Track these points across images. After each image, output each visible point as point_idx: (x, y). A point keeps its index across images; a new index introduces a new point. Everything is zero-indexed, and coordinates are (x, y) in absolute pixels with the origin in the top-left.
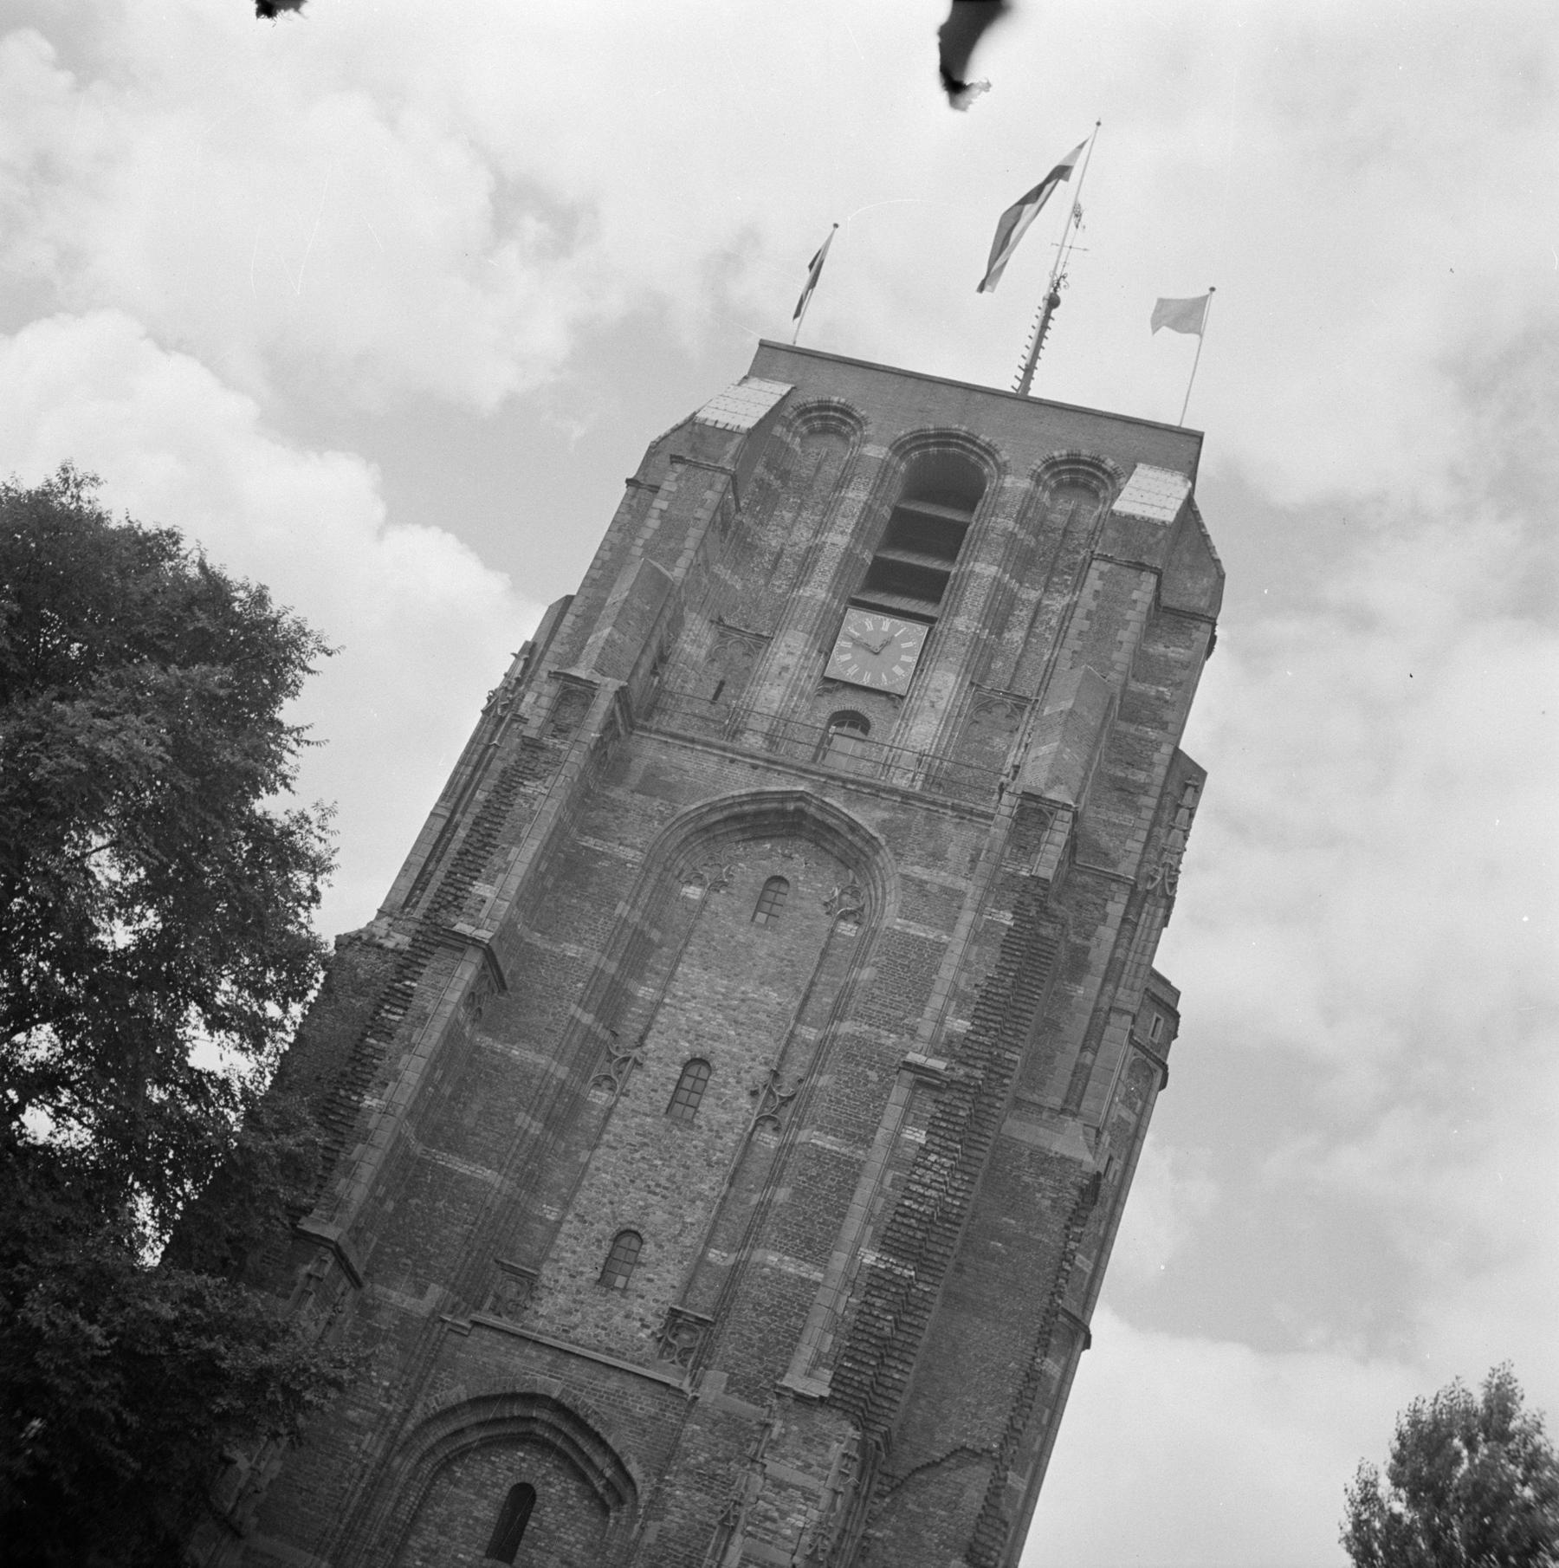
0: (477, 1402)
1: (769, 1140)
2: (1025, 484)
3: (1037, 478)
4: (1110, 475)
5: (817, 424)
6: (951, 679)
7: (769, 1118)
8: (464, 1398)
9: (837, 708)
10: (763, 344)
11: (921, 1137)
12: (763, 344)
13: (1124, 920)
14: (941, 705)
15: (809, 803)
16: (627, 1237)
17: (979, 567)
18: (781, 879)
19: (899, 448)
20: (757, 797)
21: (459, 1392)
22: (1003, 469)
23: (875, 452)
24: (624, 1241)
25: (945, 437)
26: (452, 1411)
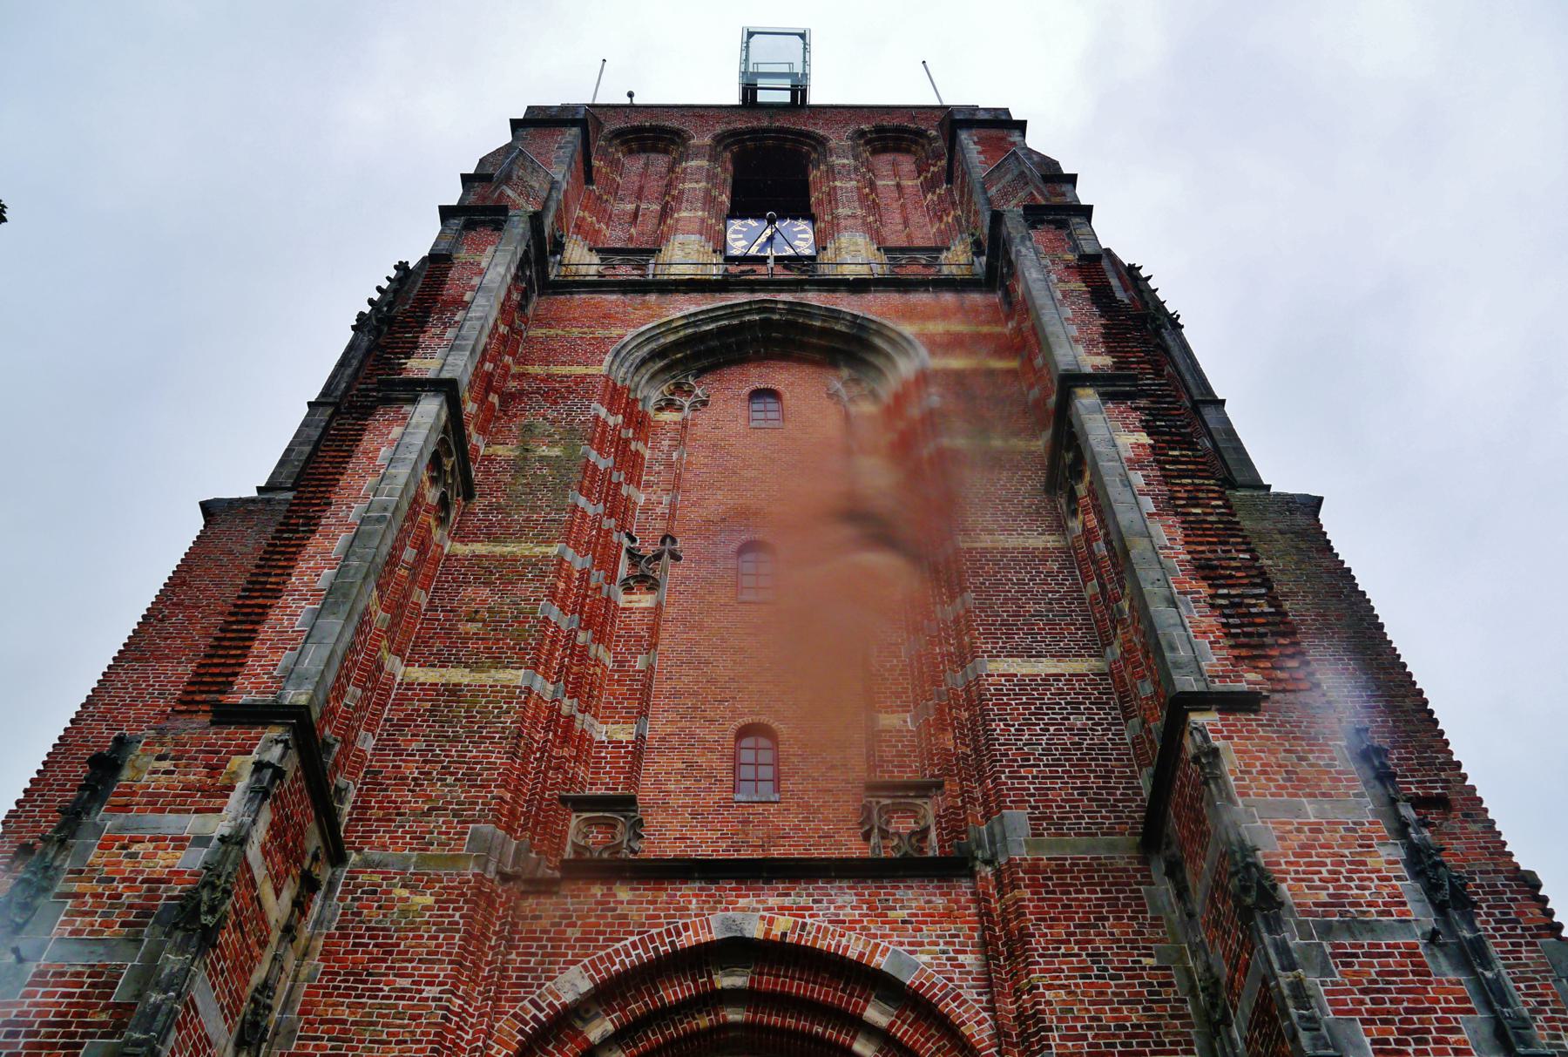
8: (585, 986)
15: (773, 311)
21: (573, 984)
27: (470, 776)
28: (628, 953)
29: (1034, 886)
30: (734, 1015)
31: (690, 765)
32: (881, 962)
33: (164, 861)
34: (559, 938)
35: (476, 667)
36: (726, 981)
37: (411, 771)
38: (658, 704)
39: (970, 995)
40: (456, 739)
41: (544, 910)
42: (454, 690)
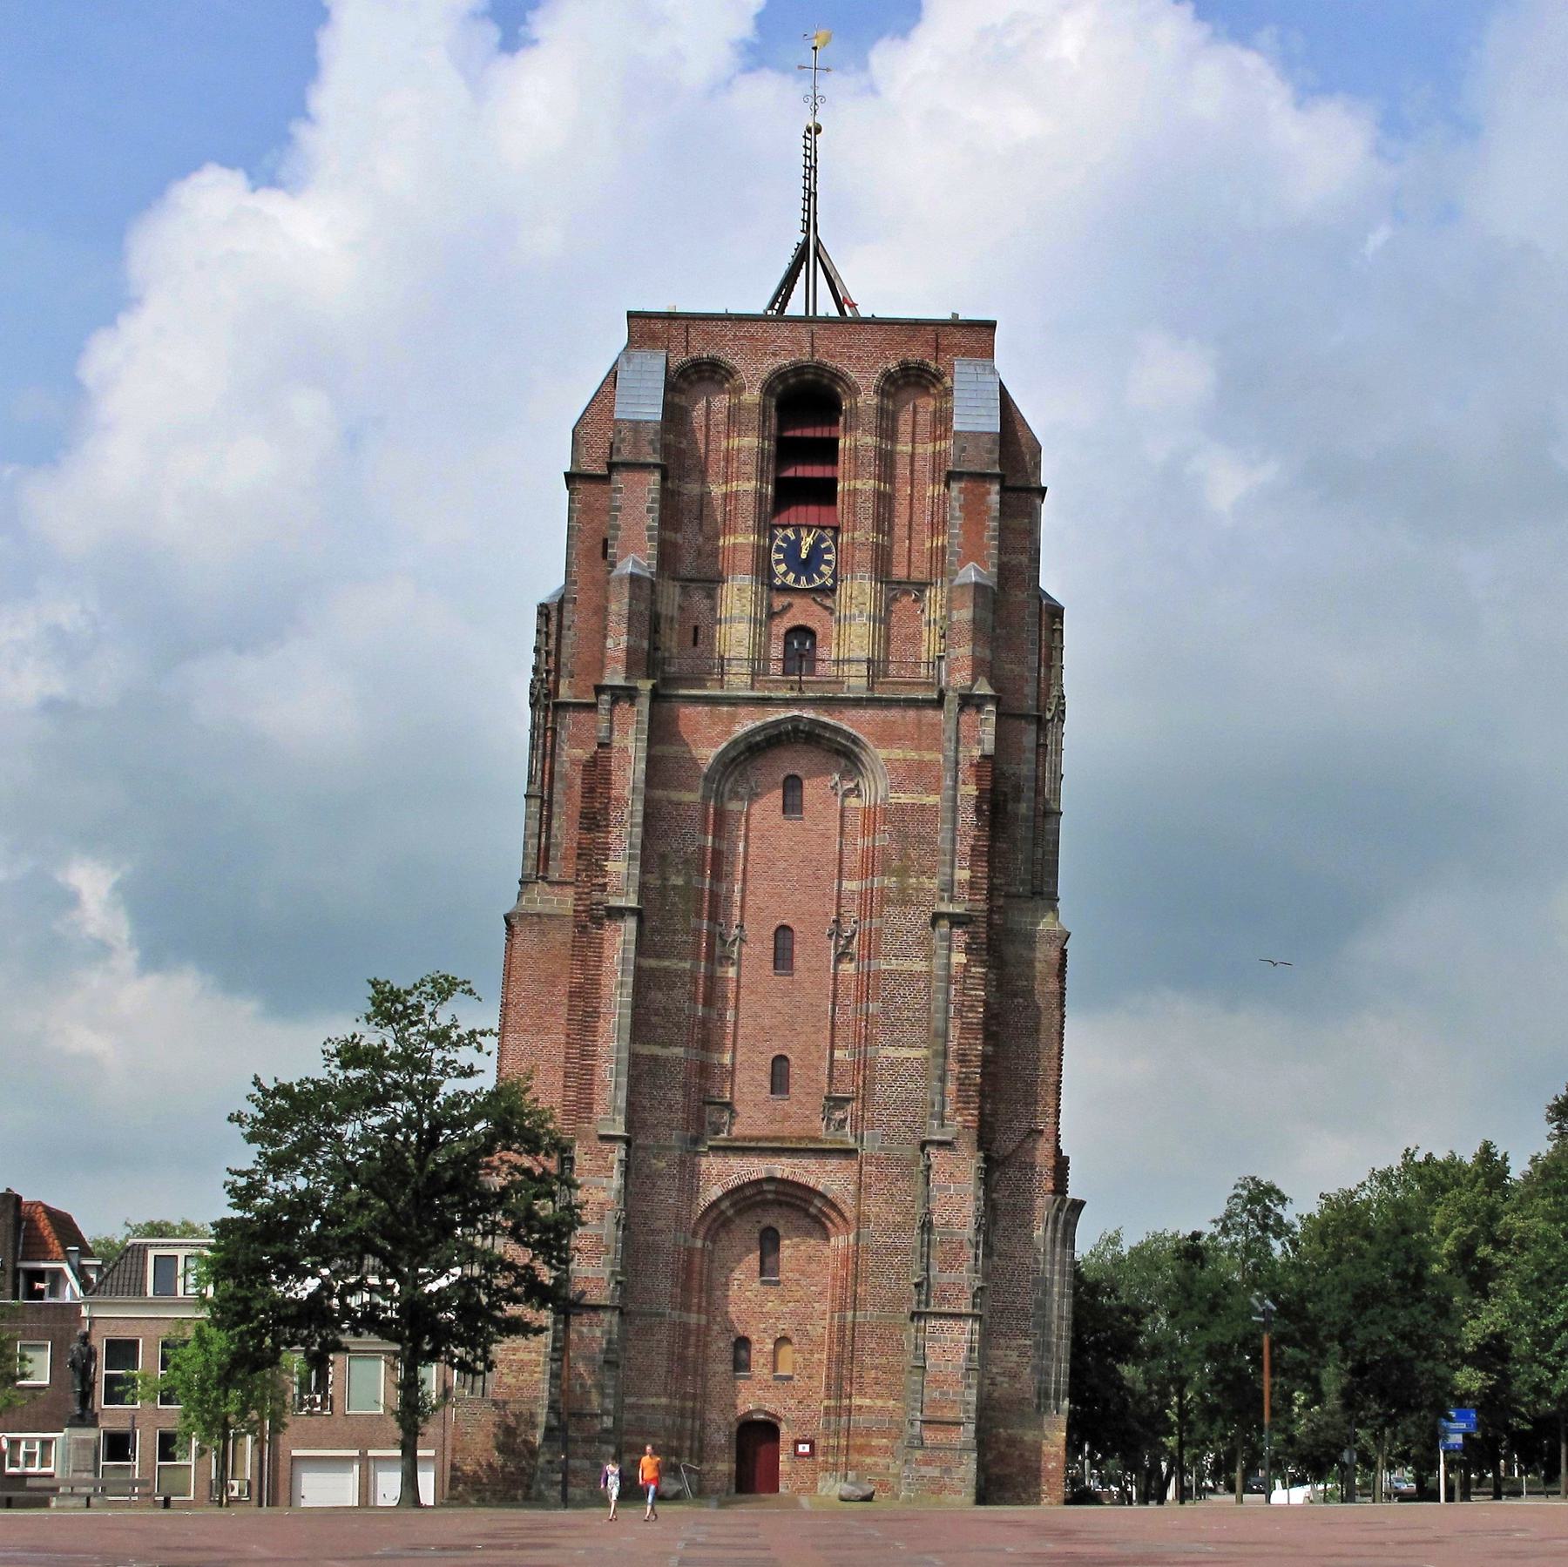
0: (729, 1194)
1: (848, 968)
2: (874, 401)
3: (882, 392)
4: (934, 376)
5: (694, 377)
6: (868, 585)
7: (843, 953)
9: (790, 625)
10: (631, 316)
11: (959, 958)
12: (631, 316)
13: (1038, 745)
14: (869, 608)
16: (780, 1062)
17: (859, 485)
18: (795, 777)
19: (768, 389)
20: (764, 728)
21: (715, 1192)
22: (854, 391)
23: (752, 396)
24: (778, 1064)
25: (798, 369)
26: (714, 1204)
27: (670, 1106)
28: (733, 1182)
29: (877, 1166)
30: (770, 1196)
31: (753, 1079)
32: (820, 1188)
33: (602, 1196)
34: (709, 1174)
35: (664, 1045)
36: (766, 1187)
37: (646, 1103)
38: (740, 1041)
39: (849, 1201)
40: (661, 1088)
41: (704, 1162)
42: (655, 1058)
